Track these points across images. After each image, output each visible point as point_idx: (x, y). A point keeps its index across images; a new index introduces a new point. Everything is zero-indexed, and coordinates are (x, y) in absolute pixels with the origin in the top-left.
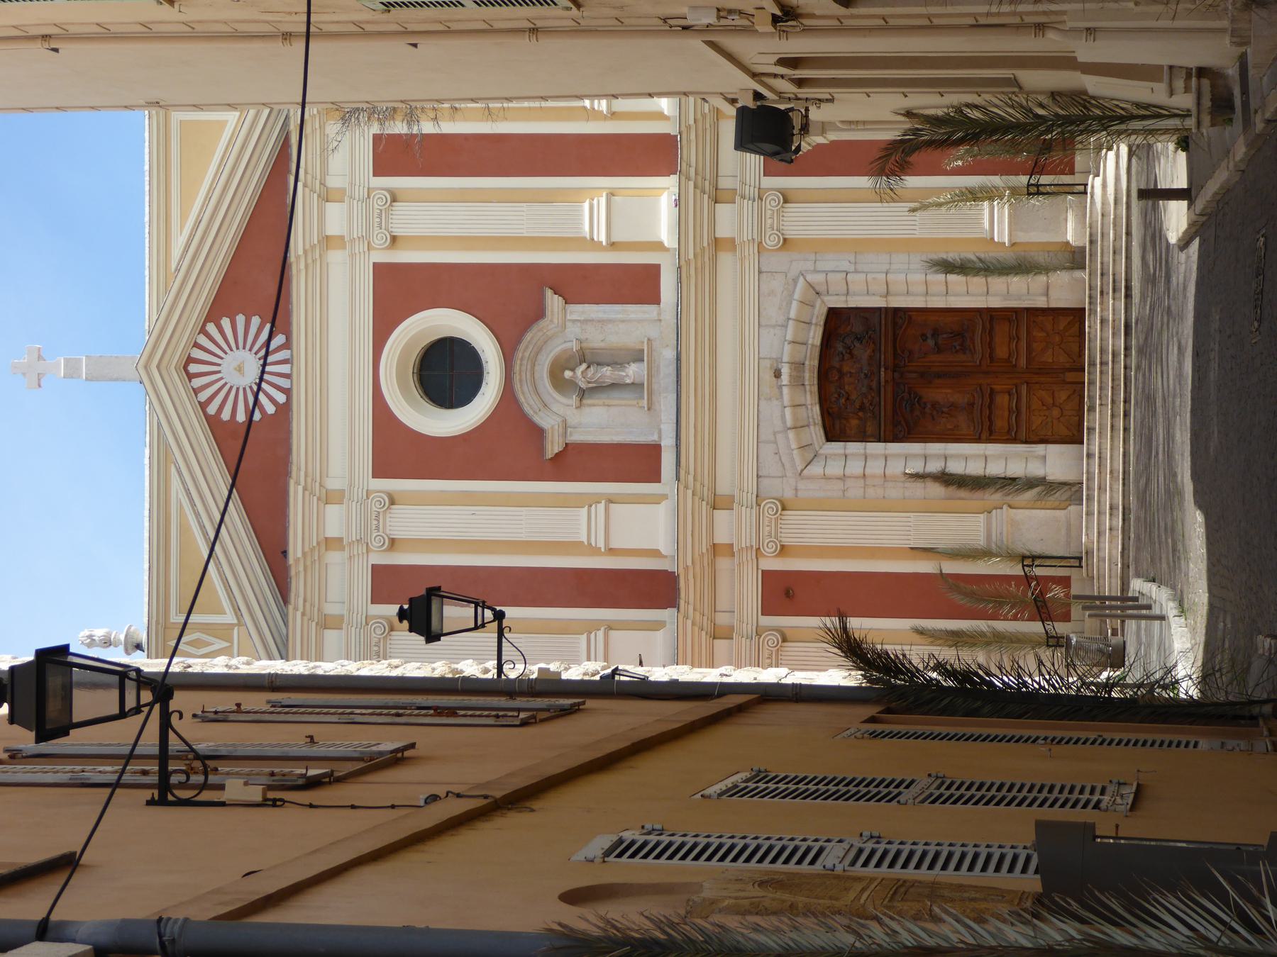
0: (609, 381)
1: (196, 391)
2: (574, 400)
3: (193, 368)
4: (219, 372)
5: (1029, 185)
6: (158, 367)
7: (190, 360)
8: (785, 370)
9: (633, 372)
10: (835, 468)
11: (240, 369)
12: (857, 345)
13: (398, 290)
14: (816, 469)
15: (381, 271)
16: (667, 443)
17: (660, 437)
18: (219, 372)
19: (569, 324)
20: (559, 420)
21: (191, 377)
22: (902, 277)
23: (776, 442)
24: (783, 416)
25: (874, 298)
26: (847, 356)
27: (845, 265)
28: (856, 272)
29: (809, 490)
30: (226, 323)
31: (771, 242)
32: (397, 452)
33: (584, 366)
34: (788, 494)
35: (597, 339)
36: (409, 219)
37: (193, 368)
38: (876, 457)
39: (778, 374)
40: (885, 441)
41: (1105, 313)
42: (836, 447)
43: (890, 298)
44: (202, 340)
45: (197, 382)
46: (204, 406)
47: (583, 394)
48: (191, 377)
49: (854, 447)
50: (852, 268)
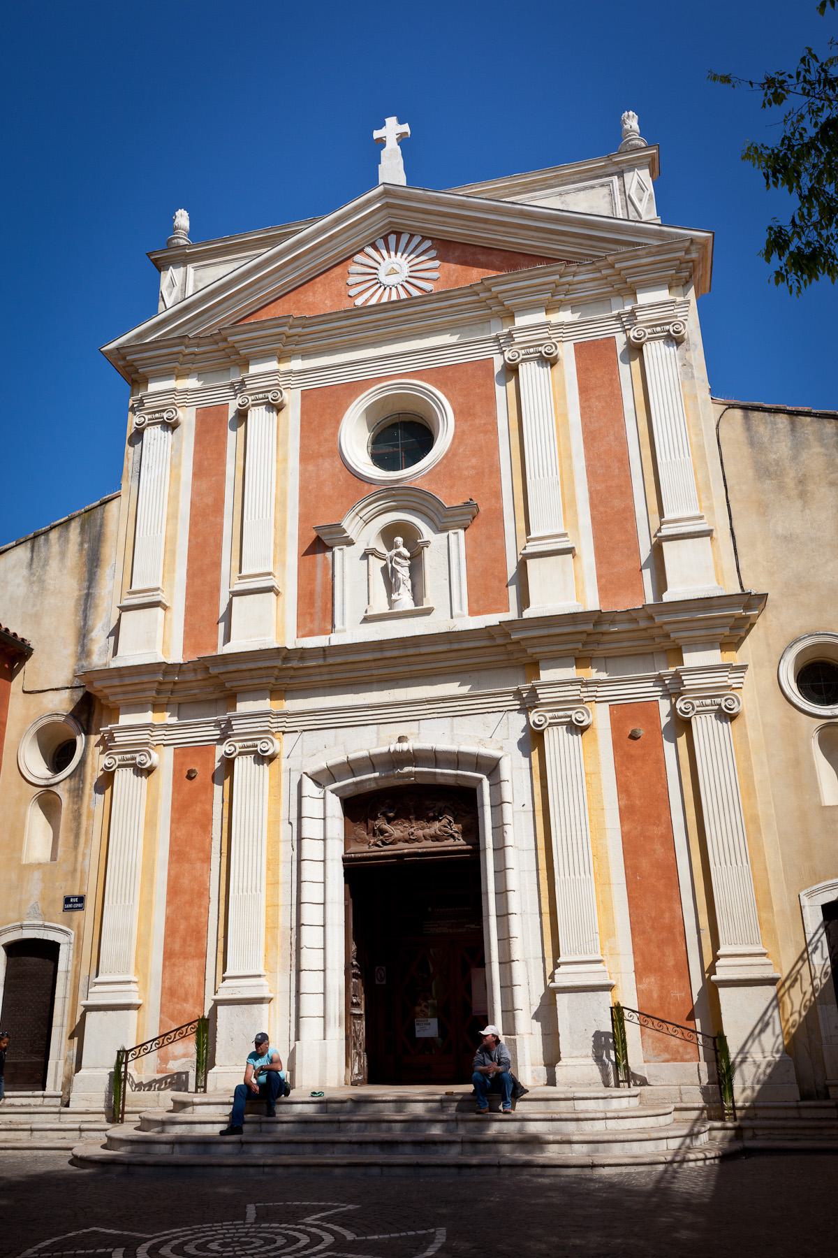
3: (392, 238)
7: (399, 234)
8: (404, 746)
9: (405, 600)
10: (312, 807)
11: (393, 272)
14: (309, 787)
21: (385, 239)
32: (322, 409)
35: (432, 560)
37: (392, 238)
39: (401, 739)
40: (344, 860)
44: (417, 240)
45: (380, 243)
48: (385, 239)
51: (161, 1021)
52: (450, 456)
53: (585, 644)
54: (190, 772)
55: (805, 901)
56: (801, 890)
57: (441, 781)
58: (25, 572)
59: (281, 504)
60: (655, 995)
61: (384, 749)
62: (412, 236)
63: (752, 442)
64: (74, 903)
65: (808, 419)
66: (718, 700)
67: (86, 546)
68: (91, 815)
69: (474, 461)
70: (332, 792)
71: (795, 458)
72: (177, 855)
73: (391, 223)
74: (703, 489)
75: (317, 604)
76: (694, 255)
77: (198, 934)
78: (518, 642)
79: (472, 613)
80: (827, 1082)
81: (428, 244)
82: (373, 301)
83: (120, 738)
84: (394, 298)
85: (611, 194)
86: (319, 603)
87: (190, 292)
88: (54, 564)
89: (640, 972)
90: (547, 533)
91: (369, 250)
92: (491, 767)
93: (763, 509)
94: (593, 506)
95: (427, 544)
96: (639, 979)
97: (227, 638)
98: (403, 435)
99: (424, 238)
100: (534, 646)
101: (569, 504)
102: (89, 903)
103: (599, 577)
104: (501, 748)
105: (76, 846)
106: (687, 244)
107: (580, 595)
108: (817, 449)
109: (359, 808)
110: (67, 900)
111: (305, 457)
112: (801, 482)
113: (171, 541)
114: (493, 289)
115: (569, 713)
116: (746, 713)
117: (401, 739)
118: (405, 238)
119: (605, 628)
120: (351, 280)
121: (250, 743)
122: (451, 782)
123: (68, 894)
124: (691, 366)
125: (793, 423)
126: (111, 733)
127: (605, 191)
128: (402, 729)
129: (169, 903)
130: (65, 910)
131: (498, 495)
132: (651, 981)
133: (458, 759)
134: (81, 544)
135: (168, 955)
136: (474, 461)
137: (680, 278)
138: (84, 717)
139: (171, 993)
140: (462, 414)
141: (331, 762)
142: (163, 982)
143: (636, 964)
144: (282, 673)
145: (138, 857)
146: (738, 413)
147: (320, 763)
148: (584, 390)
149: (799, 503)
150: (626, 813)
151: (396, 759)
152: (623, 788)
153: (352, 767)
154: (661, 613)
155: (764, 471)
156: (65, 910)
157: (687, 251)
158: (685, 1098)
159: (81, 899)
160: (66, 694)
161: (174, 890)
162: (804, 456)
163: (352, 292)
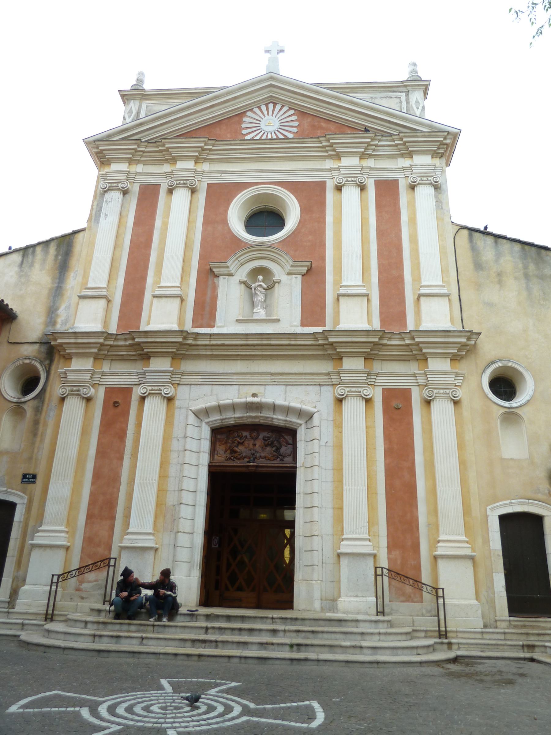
0: (255, 300)
1: (259, 107)
2: (244, 278)
3: (271, 106)
4: (268, 115)
5: (382, 568)
6: (271, 86)
7: (275, 104)
8: (256, 400)
12: (274, 449)
13: (312, 195)
14: (192, 419)
15: (322, 185)
16: (215, 331)
17: (218, 327)
18: (268, 115)
19: (289, 277)
20: (232, 272)
21: (267, 105)
22: (316, 476)
23: (211, 395)
24: (228, 399)
25: (303, 458)
26: (267, 442)
27: (324, 440)
28: (320, 446)
29: (179, 416)
30: (294, 118)
31: (340, 391)
32: (219, 195)
33: (265, 286)
34: (177, 403)
36: (351, 194)
37: (271, 106)
38: (198, 459)
39: (254, 395)
40: (210, 466)
41: (281, 634)
42: (206, 433)
43: (302, 468)
45: (263, 108)
46: (251, 110)
47: (248, 287)
48: (267, 105)
49: (206, 445)
50: (323, 443)
51: (81, 558)
52: (295, 233)
53: (371, 350)
54: (116, 402)
55: (489, 513)
56: (487, 506)
57: (276, 423)
58: (16, 269)
59: (188, 246)
60: (399, 562)
61: (243, 400)
62: (283, 106)
63: (474, 249)
64: (29, 479)
65: (505, 241)
66: (447, 391)
67: (60, 257)
68: (45, 425)
69: (310, 237)
70: (206, 423)
71: (497, 261)
72: (101, 453)
73: (271, 96)
74: (444, 271)
75: (205, 309)
76: (448, 141)
77: (111, 505)
78: (332, 344)
79: (303, 325)
80: (497, 618)
81: (292, 112)
82: (258, 137)
83: (71, 377)
84: (269, 137)
85: (401, 102)
86: (207, 309)
87: (142, 114)
88: (37, 266)
89: (390, 548)
90: (353, 284)
91: (256, 110)
92: (310, 416)
93: (478, 287)
94: (380, 272)
95: (279, 282)
96: (389, 552)
97: (148, 324)
98: (265, 218)
99: (290, 109)
100: (341, 347)
101: (365, 269)
102: (39, 480)
103: (381, 313)
104: (315, 407)
105: (33, 443)
106: (446, 134)
107: (369, 322)
108: (508, 258)
109: (222, 434)
110: (24, 476)
111: (206, 222)
112: (499, 274)
113: (114, 262)
114: (331, 141)
115: (359, 389)
116: (462, 401)
117: (254, 395)
118: (278, 107)
119: (385, 341)
120: (244, 125)
121: (156, 388)
122: (282, 424)
123: (25, 473)
124: (441, 202)
125: (496, 242)
126: (65, 373)
127: (398, 100)
128: (254, 390)
129: (93, 484)
130: (23, 482)
131: (323, 258)
132: (396, 553)
133: (288, 410)
134: (56, 256)
135: (90, 516)
136: (310, 237)
137: (439, 153)
138: (47, 362)
139: (89, 540)
140: (304, 210)
141: (208, 405)
142: (85, 533)
143: (388, 543)
144: (182, 348)
145: (73, 452)
146: (466, 232)
147: (201, 405)
148: (379, 206)
149: (497, 286)
150: (388, 452)
151: (250, 407)
152: (387, 437)
153: (220, 409)
154: (419, 337)
155: (478, 266)
156: (23, 482)
157: (445, 138)
158: (416, 624)
159: (34, 477)
160: (37, 347)
161: (97, 475)
162: (502, 261)
163: (244, 132)
